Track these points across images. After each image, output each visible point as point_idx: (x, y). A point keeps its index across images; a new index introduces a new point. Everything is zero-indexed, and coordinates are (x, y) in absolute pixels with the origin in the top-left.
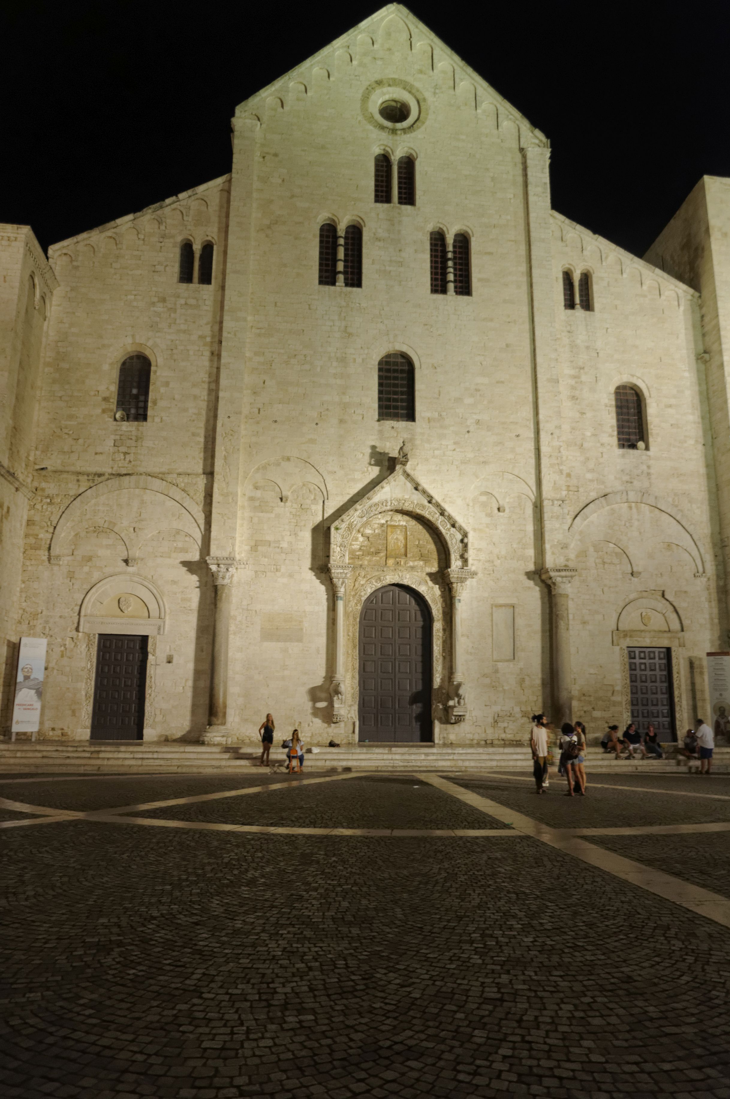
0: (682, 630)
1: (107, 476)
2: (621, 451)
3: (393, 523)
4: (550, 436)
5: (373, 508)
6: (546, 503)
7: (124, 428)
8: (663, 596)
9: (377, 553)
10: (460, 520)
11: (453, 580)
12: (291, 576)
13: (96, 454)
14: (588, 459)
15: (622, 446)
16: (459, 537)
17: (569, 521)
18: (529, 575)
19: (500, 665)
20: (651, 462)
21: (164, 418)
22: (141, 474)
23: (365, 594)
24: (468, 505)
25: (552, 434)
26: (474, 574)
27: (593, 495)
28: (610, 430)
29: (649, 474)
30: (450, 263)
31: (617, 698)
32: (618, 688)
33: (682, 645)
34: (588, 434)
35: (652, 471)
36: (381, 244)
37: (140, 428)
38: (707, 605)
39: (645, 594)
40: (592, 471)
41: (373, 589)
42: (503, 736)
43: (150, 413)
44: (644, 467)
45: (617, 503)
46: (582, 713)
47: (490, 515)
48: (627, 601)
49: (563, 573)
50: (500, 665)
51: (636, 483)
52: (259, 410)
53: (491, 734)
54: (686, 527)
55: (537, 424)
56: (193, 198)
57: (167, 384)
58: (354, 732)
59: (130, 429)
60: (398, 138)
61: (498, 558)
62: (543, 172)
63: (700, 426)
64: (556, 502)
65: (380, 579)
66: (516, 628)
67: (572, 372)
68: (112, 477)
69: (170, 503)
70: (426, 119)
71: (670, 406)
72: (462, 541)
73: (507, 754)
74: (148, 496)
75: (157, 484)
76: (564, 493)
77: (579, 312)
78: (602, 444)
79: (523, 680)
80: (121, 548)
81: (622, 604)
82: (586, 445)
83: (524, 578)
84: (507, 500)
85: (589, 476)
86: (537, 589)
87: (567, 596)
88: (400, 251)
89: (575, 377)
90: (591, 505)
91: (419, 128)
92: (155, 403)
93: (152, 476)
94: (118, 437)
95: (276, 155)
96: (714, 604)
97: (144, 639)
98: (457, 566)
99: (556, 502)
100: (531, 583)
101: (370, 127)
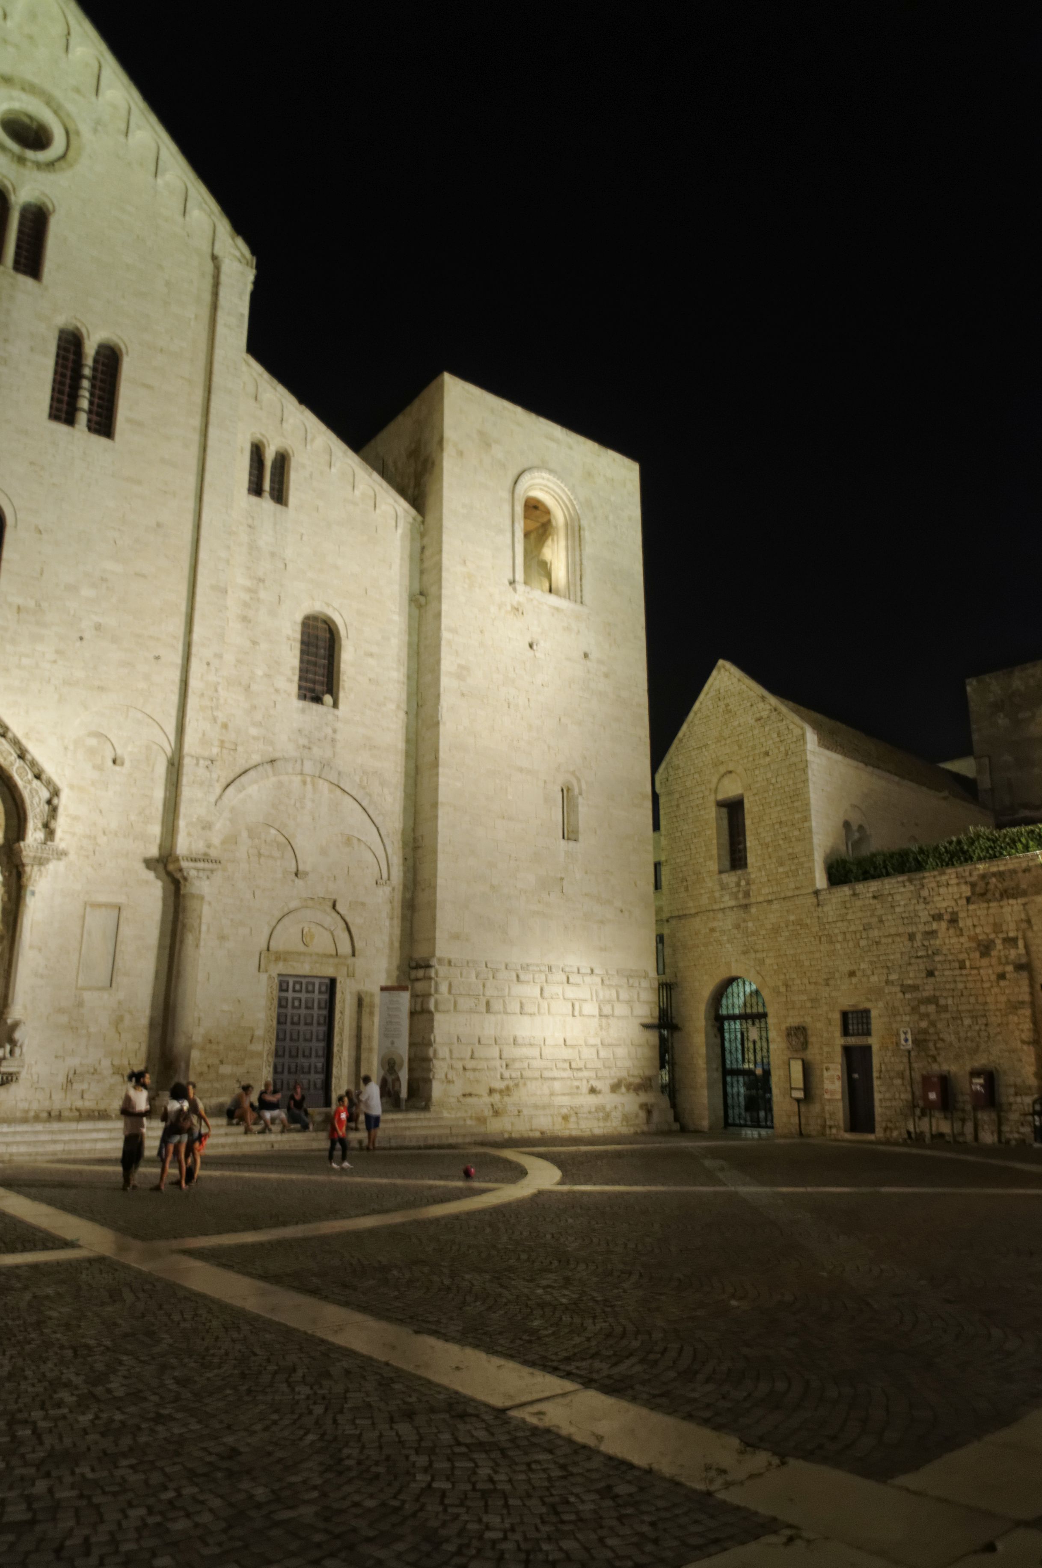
0: (354, 955)
2: (301, 704)
4: (205, 666)
6: (187, 762)
8: (334, 906)
10: (50, 770)
11: (26, 860)
14: (254, 707)
15: (302, 697)
16: (45, 794)
17: (218, 790)
18: (149, 863)
19: (87, 996)
20: (339, 725)
24: (66, 748)
26: (64, 853)
27: (256, 758)
29: (333, 740)
31: (257, 1047)
32: (260, 1032)
33: (351, 975)
34: (259, 672)
35: (338, 737)
38: (387, 923)
39: (310, 903)
40: (259, 724)
42: (79, 1104)
44: (329, 731)
45: (287, 774)
46: (205, 1069)
47: (99, 768)
48: (286, 910)
49: (200, 865)
50: (87, 996)
51: (315, 750)
53: (59, 1101)
54: (372, 817)
61: (104, 833)
63: (405, 687)
64: (201, 762)
66: (119, 939)
67: (248, 583)
71: (371, 655)
72: (49, 802)
73: (82, 1131)
76: (215, 750)
77: (266, 504)
78: (277, 691)
79: (121, 1019)
81: (278, 915)
82: (254, 687)
83: (140, 867)
84: (129, 749)
85: (253, 731)
86: (159, 884)
87: (202, 898)
89: (249, 590)
90: (252, 774)
96: (397, 922)
98: (35, 840)
100: (150, 875)
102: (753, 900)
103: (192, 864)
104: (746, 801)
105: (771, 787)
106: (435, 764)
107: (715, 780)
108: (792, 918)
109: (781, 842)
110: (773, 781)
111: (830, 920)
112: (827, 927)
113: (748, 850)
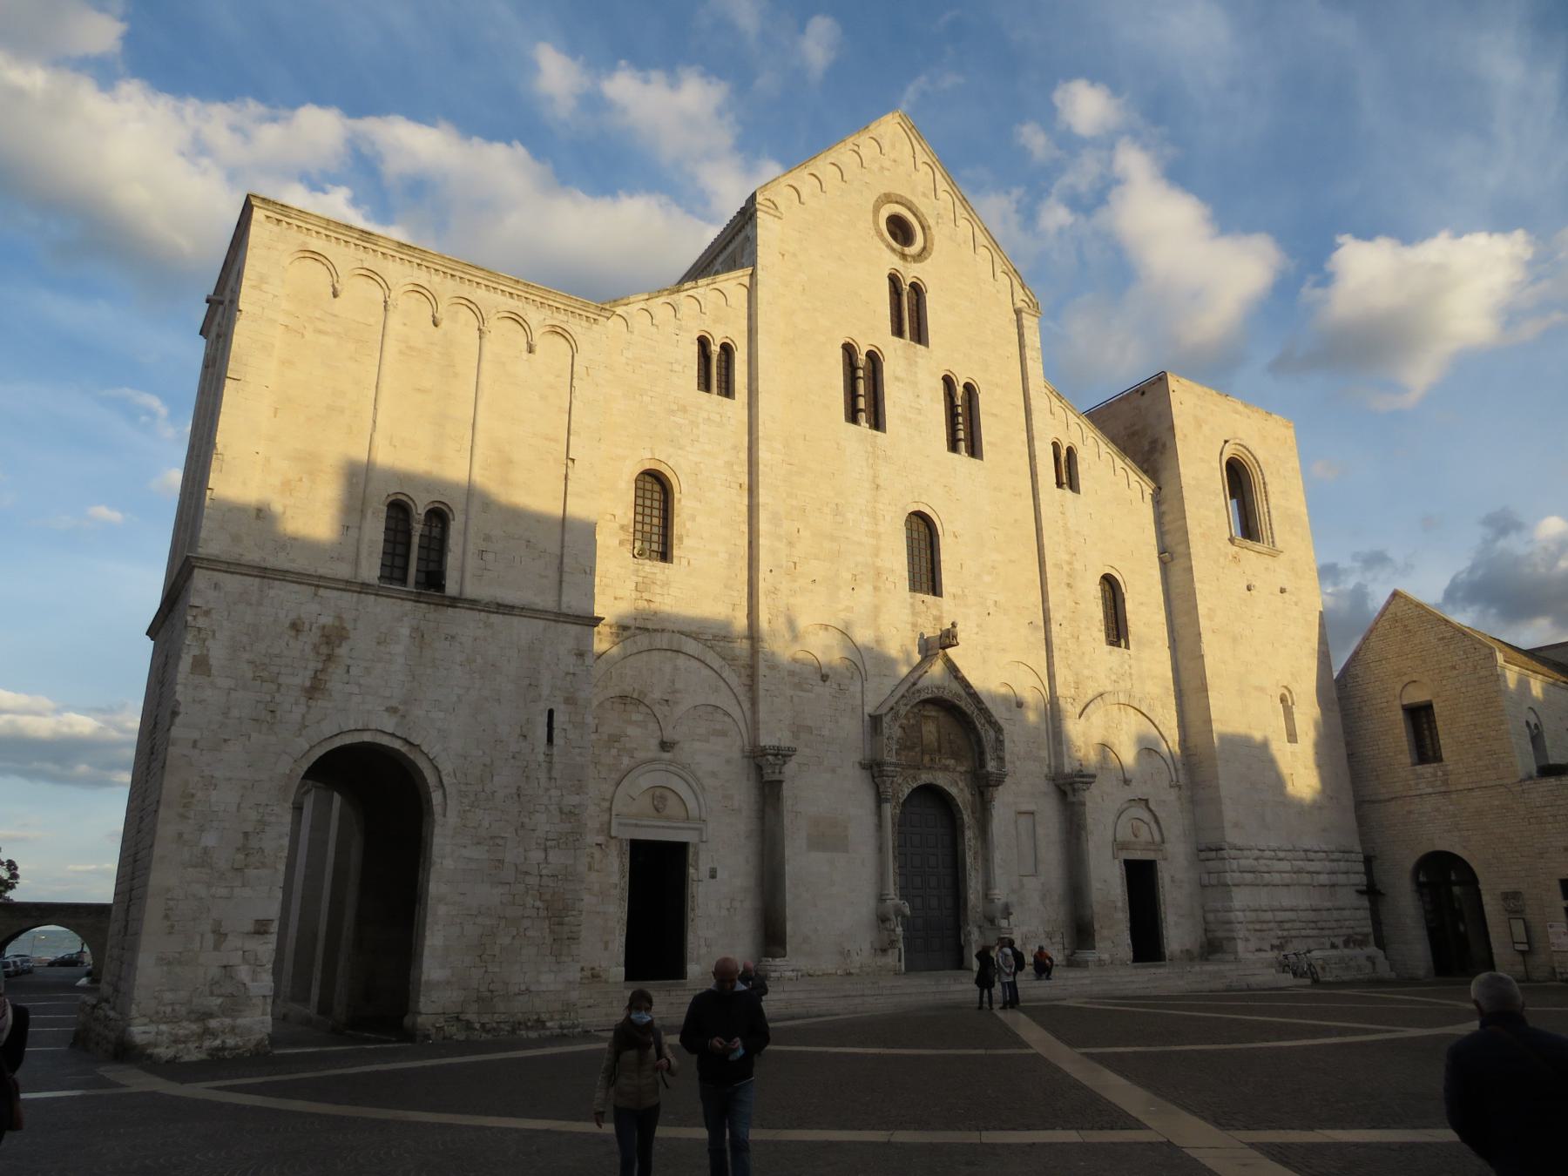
1: (632, 631)
3: (925, 713)
5: (917, 695)
7: (647, 568)
9: (912, 748)
12: (833, 771)
13: (616, 598)
20: (1132, 662)
21: (692, 562)
22: (673, 632)
23: (903, 795)
25: (1060, 625)
28: (1099, 624)
29: (1131, 674)
30: (960, 419)
32: (1120, 904)
35: (1133, 672)
36: (901, 385)
37: (666, 571)
39: (1133, 803)
41: (910, 790)
43: (676, 552)
44: (1127, 667)
49: (1085, 780)
52: (795, 563)
55: (1046, 612)
56: (711, 287)
57: (693, 518)
58: (900, 960)
59: (656, 570)
60: (908, 265)
62: (1036, 336)
65: (914, 777)
68: (637, 631)
69: (706, 672)
70: (932, 249)
71: (1142, 604)
74: (681, 661)
75: (691, 646)
77: (1068, 492)
80: (652, 726)
88: (918, 396)
90: (1092, 705)
91: (926, 258)
92: (681, 539)
93: (687, 636)
94: (640, 579)
95: (794, 255)
97: (681, 848)
99: (1069, 700)
101: (884, 247)
102: (1453, 788)
103: (1082, 780)
104: (1434, 705)
105: (1462, 695)
106: (1204, 688)
107: (1399, 687)
108: (1497, 803)
109: (1478, 741)
110: (1464, 690)
111: (1538, 804)
112: (1535, 810)
113: (1442, 747)
